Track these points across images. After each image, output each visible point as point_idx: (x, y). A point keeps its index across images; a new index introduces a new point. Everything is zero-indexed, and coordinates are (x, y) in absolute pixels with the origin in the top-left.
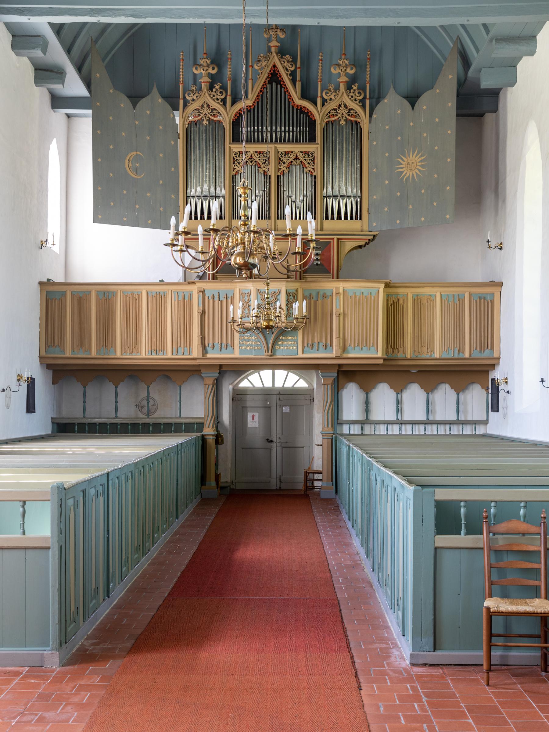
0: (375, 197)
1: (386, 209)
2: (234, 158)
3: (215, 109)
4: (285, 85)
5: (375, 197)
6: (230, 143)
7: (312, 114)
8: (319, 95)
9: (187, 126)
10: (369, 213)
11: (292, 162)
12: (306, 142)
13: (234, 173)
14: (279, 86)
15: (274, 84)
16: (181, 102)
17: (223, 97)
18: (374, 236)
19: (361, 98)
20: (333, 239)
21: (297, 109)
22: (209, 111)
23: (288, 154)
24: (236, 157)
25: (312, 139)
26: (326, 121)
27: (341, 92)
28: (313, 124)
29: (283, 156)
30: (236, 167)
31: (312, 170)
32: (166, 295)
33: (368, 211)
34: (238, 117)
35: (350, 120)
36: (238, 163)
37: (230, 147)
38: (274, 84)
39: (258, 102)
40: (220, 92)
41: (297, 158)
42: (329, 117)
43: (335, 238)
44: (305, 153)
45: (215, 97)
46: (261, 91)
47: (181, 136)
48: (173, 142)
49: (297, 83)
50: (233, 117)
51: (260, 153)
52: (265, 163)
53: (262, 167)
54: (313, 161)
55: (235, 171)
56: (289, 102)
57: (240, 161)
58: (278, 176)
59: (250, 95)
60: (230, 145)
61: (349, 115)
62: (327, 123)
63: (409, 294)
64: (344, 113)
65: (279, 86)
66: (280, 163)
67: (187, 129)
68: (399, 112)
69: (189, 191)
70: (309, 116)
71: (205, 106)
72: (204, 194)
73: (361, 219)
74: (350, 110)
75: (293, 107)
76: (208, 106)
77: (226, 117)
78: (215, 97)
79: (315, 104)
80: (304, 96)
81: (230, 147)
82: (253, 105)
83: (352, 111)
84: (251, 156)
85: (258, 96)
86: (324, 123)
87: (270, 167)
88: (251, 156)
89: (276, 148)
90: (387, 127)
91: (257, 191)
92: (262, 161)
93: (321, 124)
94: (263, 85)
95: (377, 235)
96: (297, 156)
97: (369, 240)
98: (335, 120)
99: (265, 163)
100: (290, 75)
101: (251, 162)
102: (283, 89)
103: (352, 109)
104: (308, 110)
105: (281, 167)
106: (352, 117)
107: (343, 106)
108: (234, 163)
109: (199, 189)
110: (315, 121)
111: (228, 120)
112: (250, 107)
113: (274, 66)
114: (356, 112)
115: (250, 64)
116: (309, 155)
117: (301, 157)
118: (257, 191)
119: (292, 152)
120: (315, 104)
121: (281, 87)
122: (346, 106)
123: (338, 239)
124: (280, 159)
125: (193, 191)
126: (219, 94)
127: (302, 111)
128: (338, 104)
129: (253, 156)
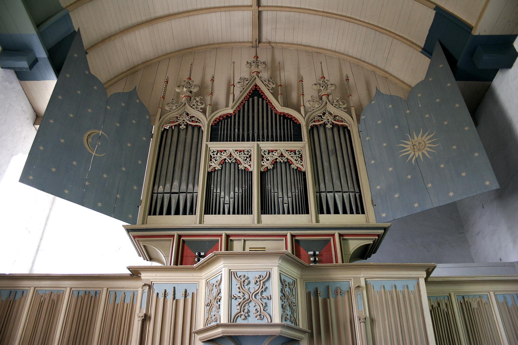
0: (378, 187)
1: (396, 196)
2: (211, 156)
3: (193, 117)
4: (267, 98)
5: (378, 187)
6: (207, 141)
7: (296, 119)
8: (302, 104)
9: (163, 129)
10: (374, 205)
11: (276, 159)
12: (291, 141)
13: (210, 170)
14: (260, 99)
15: (256, 98)
16: (160, 110)
17: (203, 106)
18: (385, 229)
19: (345, 106)
20: (333, 235)
21: (280, 116)
22: (187, 118)
23: (272, 152)
24: (214, 155)
25: (298, 138)
26: (311, 124)
27: (324, 102)
28: (298, 127)
29: (266, 153)
30: (213, 164)
31: (301, 167)
32: (97, 296)
33: (372, 203)
34: (218, 123)
35: (336, 124)
36: (216, 160)
37: (207, 145)
38: (256, 98)
39: (239, 111)
40: (201, 103)
41: (282, 155)
42: (314, 122)
43: (336, 233)
44: (291, 151)
45: (195, 106)
46: (242, 103)
47: (155, 136)
48: (144, 139)
49: (279, 96)
50: (212, 122)
51: (240, 151)
52: (246, 160)
53: (243, 164)
54: (301, 158)
55: (211, 168)
56: (272, 111)
57: (218, 158)
58: (261, 172)
59: (231, 104)
60: (207, 143)
61: (335, 120)
62: (312, 127)
63: (452, 294)
64: (329, 119)
65: (260, 99)
66: (263, 160)
67: (163, 133)
68: (390, 106)
69: (156, 187)
70: (293, 121)
71: (184, 114)
72: (174, 190)
73: (363, 213)
74: (335, 116)
75: (276, 114)
76: (188, 114)
77: (205, 123)
78: (195, 106)
79: (299, 112)
80: (286, 104)
81: (207, 145)
82: (234, 112)
83: (337, 117)
84: (231, 154)
85: (239, 106)
86: (310, 126)
87: (252, 163)
88: (231, 154)
89: (257, 144)
90: (379, 122)
91: (236, 188)
92: (243, 158)
93: (307, 125)
94: (245, 99)
95: (389, 227)
96: (282, 154)
97: (378, 235)
98: (320, 125)
99: (246, 160)
100: (271, 90)
101: (230, 159)
102: (265, 101)
103: (337, 116)
104: (291, 116)
105: (265, 164)
106: (338, 121)
107: (327, 113)
108: (211, 160)
109: (168, 186)
110: (300, 124)
111: (206, 123)
112: (231, 114)
113: (256, 85)
114: (342, 118)
115: (232, 83)
116: (295, 154)
117: (287, 155)
118: (236, 188)
119: (277, 151)
120: (299, 112)
121: (263, 100)
122: (331, 114)
123: (340, 235)
124: (263, 157)
125: (161, 187)
126: (199, 104)
127: (285, 117)
128: (322, 111)
129: (233, 154)
